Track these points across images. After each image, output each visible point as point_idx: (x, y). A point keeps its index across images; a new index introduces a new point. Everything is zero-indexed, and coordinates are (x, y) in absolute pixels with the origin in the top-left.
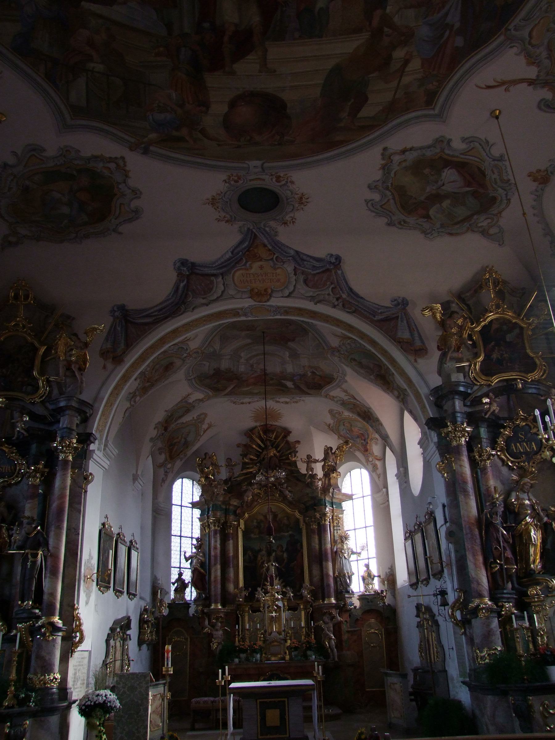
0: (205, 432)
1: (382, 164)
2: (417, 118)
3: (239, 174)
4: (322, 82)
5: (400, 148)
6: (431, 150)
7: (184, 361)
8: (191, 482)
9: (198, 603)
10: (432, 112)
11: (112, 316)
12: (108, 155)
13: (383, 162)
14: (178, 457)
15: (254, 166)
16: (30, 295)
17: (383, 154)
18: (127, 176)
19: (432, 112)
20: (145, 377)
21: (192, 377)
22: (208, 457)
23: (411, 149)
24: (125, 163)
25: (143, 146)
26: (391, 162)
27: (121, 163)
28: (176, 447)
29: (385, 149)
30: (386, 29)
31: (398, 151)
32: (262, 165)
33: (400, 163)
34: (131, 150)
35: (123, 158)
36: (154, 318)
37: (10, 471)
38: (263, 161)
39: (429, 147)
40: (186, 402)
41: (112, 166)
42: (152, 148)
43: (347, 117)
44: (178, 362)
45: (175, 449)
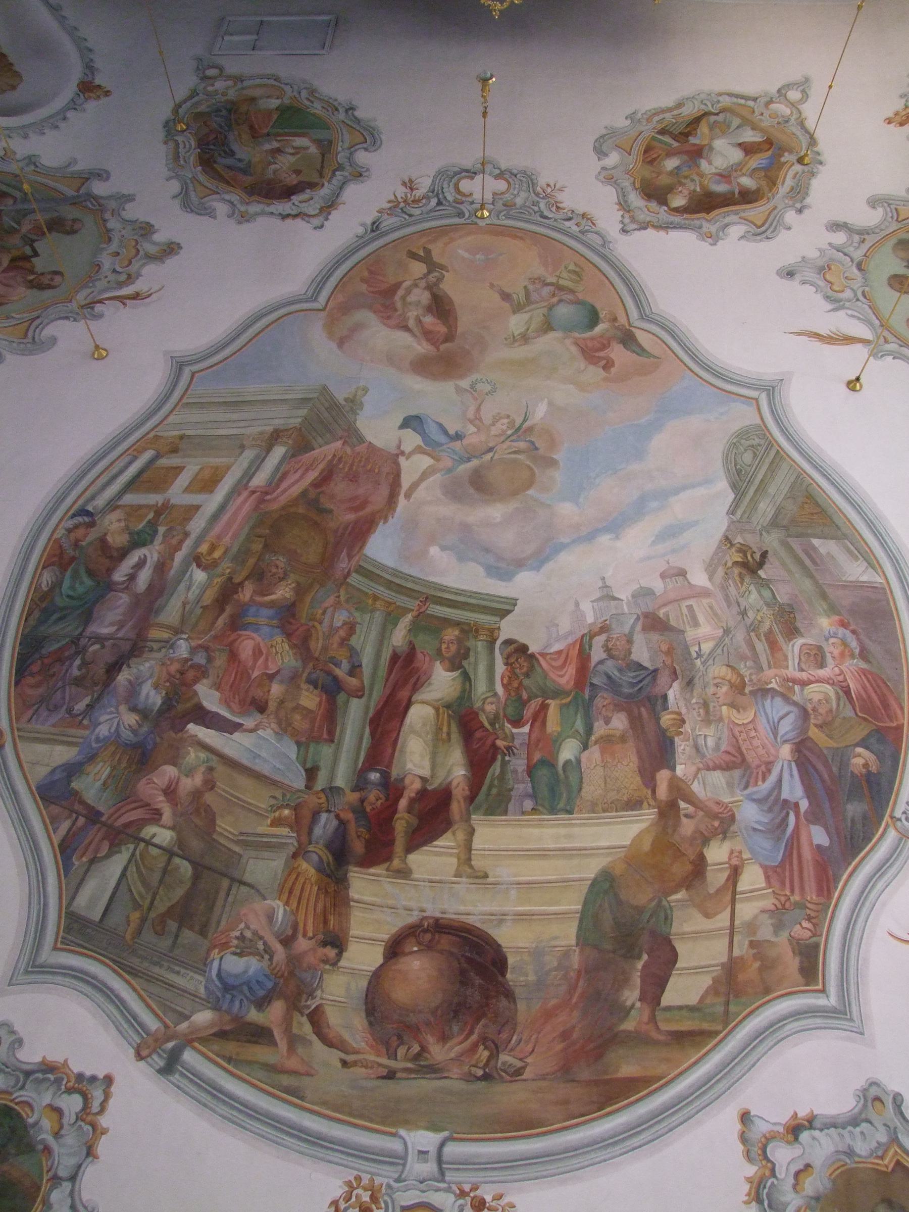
1: (749, 1180)
2: (796, 1015)
3: (378, 1180)
4: (579, 907)
5: (784, 1117)
6: (862, 1133)
10: (821, 1001)
12: (76, 1067)
13: (751, 1170)
15: (420, 1152)
17: (743, 1139)
18: (90, 1152)
19: (821, 1001)
23: (810, 1122)
24: (107, 1096)
25: (170, 1045)
26: (773, 1173)
27: (97, 1095)
29: (745, 1117)
30: (682, 805)
31: (781, 1129)
32: (442, 1145)
33: (797, 1174)
34: (139, 1057)
35: (109, 1080)
38: (446, 1134)
39: (855, 1121)
41: (72, 1104)
42: (188, 1056)
43: (638, 1004)
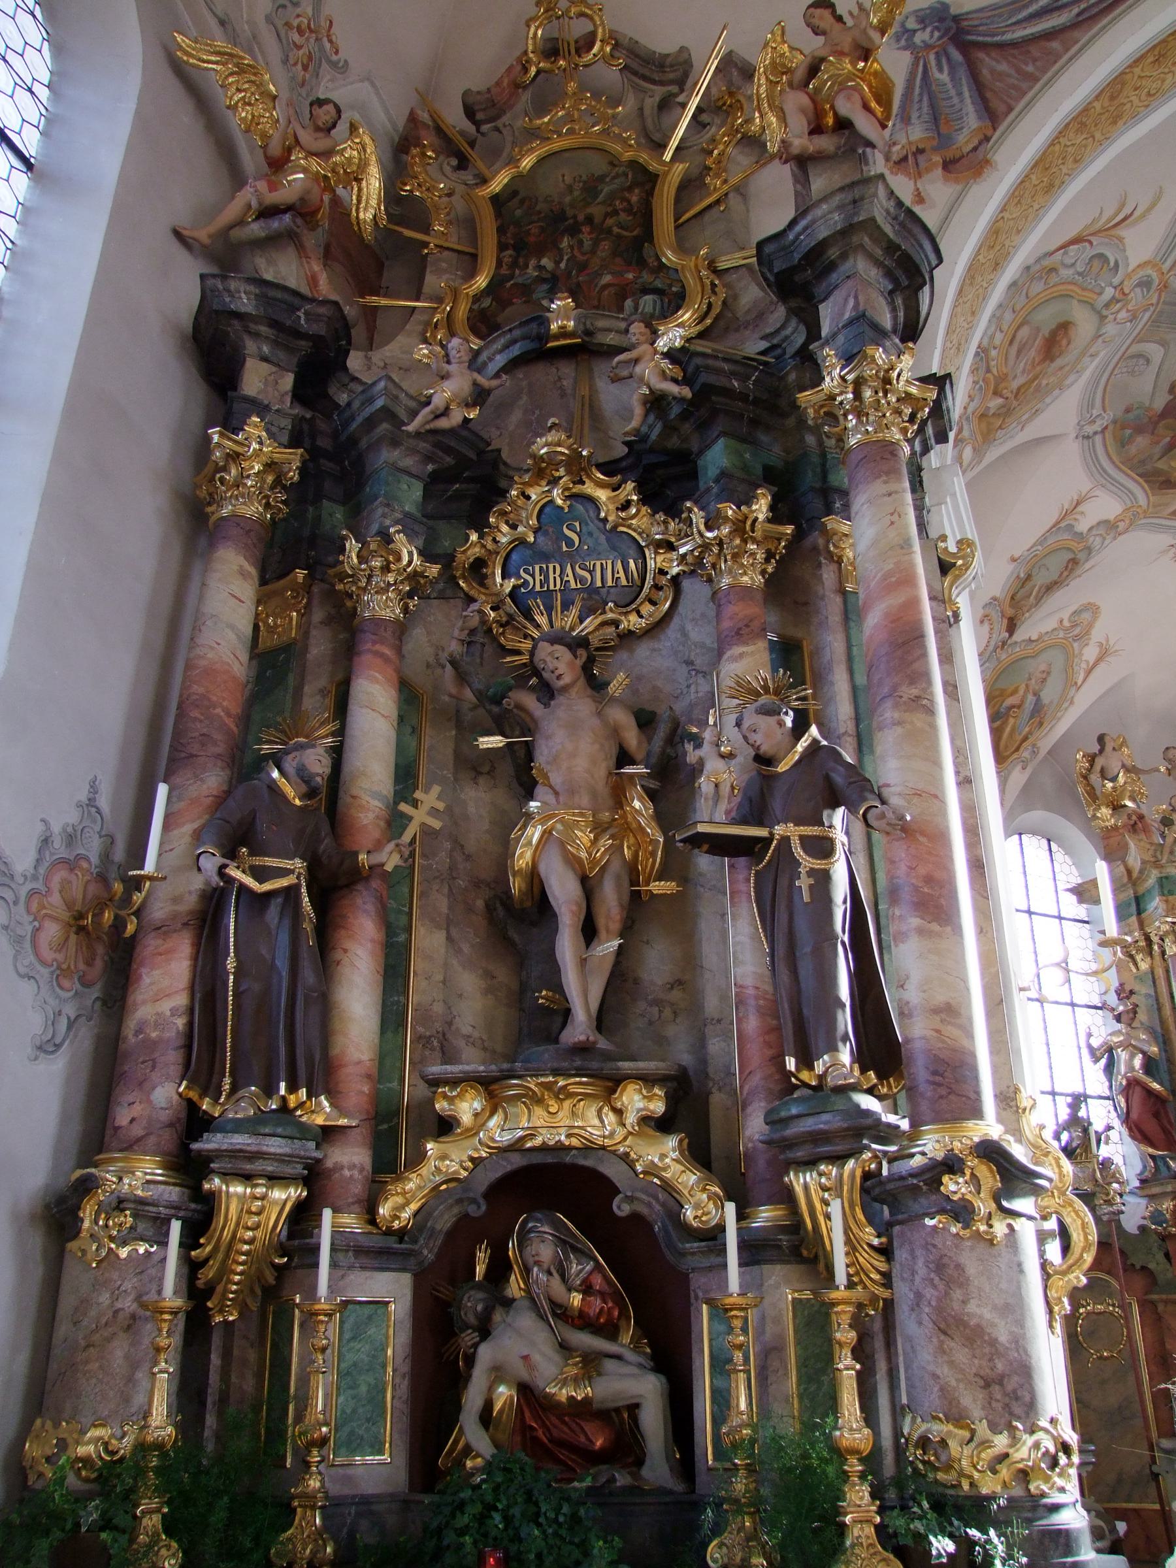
0: (1089, 672)
7: (1103, 318)
8: (1045, 842)
9: (1156, 1190)
11: (905, 48)
14: (1015, 756)
16: (600, 30)
20: (988, 371)
21: (1097, 427)
22: (1109, 748)
28: (1011, 721)
36: (1076, 11)
37: (624, 582)
40: (1070, 527)
44: (1084, 324)
45: (1008, 730)
